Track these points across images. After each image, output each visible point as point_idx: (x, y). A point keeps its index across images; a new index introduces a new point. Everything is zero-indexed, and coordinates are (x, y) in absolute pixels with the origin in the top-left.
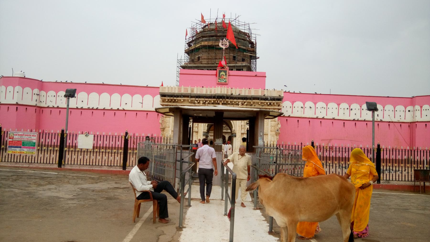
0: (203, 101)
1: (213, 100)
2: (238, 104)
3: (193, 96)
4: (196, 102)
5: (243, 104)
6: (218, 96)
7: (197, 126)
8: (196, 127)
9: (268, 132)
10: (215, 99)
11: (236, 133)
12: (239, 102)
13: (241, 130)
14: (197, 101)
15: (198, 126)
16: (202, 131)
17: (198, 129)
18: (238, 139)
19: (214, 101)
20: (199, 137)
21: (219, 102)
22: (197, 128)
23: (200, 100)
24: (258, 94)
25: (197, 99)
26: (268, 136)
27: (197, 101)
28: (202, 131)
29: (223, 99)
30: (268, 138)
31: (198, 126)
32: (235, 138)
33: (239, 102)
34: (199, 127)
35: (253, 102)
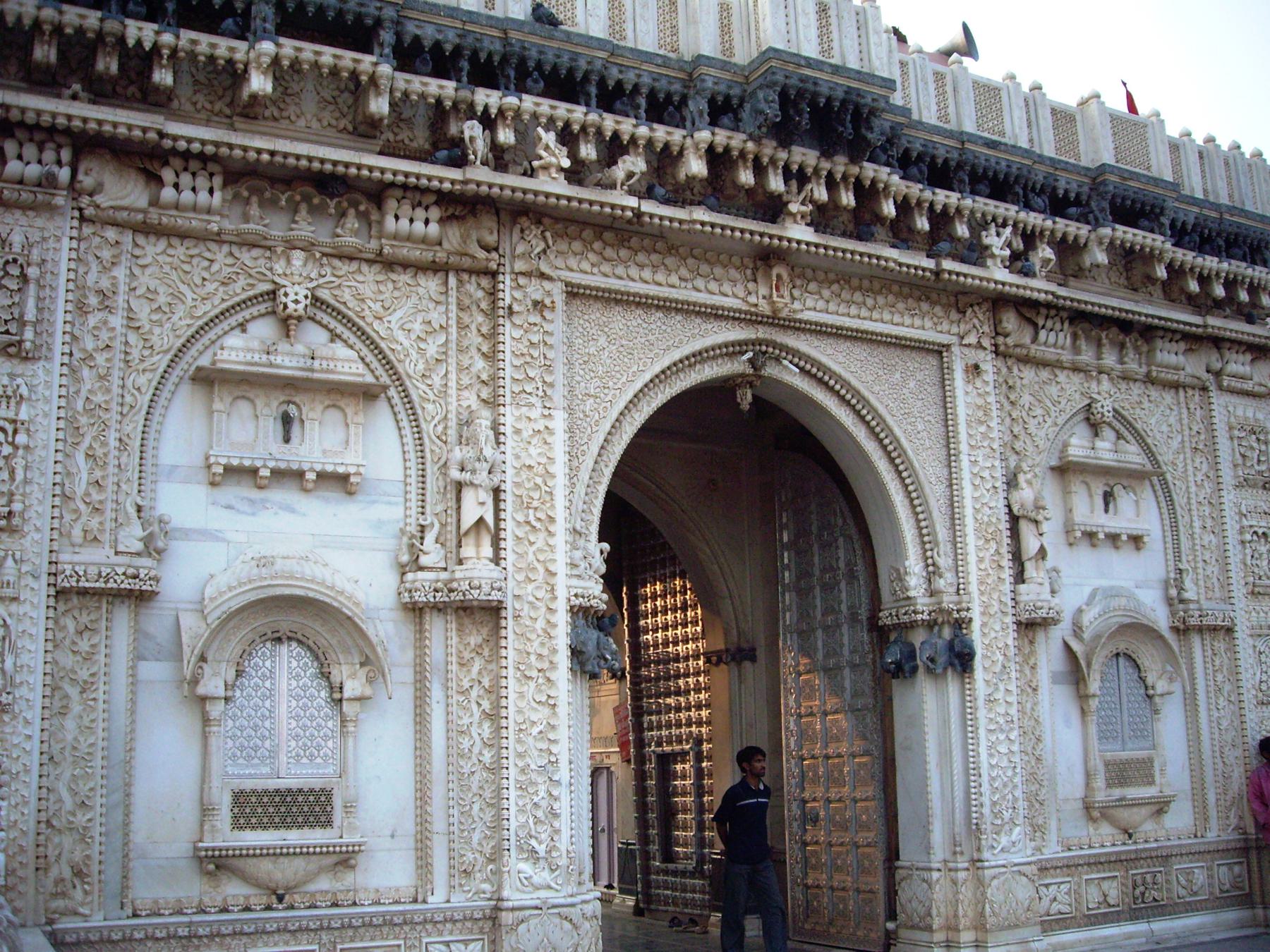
0: (568, 137)
1: (711, 149)
2: (975, 253)
3: (429, 34)
4: (472, 130)
5: (1018, 261)
6: (801, 93)
7: (490, 519)
8: (481, 521)
9: (1228, 599)
10: (737, 141)
11: (960, 625)
12: (980, 224)
13: (1007, 574)
14: (488, 122)
15: (497, 519)
16: (562, 593)
17: (497, 560)
18: (990, 701)
19: (718, 159)
20: (512, 685)
21: (776, 183)
22: (487, 551)
23: (535, 116)
24: (1148, 168)
25: (486, 98)
26: (1232, 649)
27: (488, 122)
28: (562, 593)
29: (827, 154)
30: (1235, 672)
31: (497, 519)
32: (952, 686)
33: (980, 224)
34: (509, 526)
35: (1111, 247)
